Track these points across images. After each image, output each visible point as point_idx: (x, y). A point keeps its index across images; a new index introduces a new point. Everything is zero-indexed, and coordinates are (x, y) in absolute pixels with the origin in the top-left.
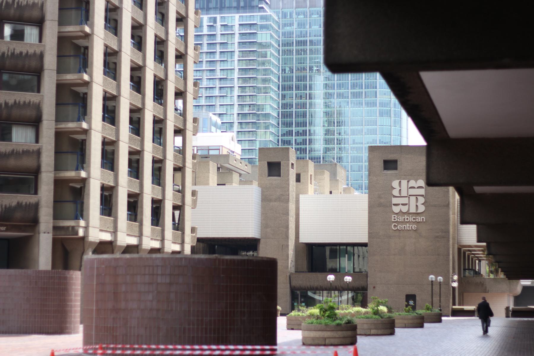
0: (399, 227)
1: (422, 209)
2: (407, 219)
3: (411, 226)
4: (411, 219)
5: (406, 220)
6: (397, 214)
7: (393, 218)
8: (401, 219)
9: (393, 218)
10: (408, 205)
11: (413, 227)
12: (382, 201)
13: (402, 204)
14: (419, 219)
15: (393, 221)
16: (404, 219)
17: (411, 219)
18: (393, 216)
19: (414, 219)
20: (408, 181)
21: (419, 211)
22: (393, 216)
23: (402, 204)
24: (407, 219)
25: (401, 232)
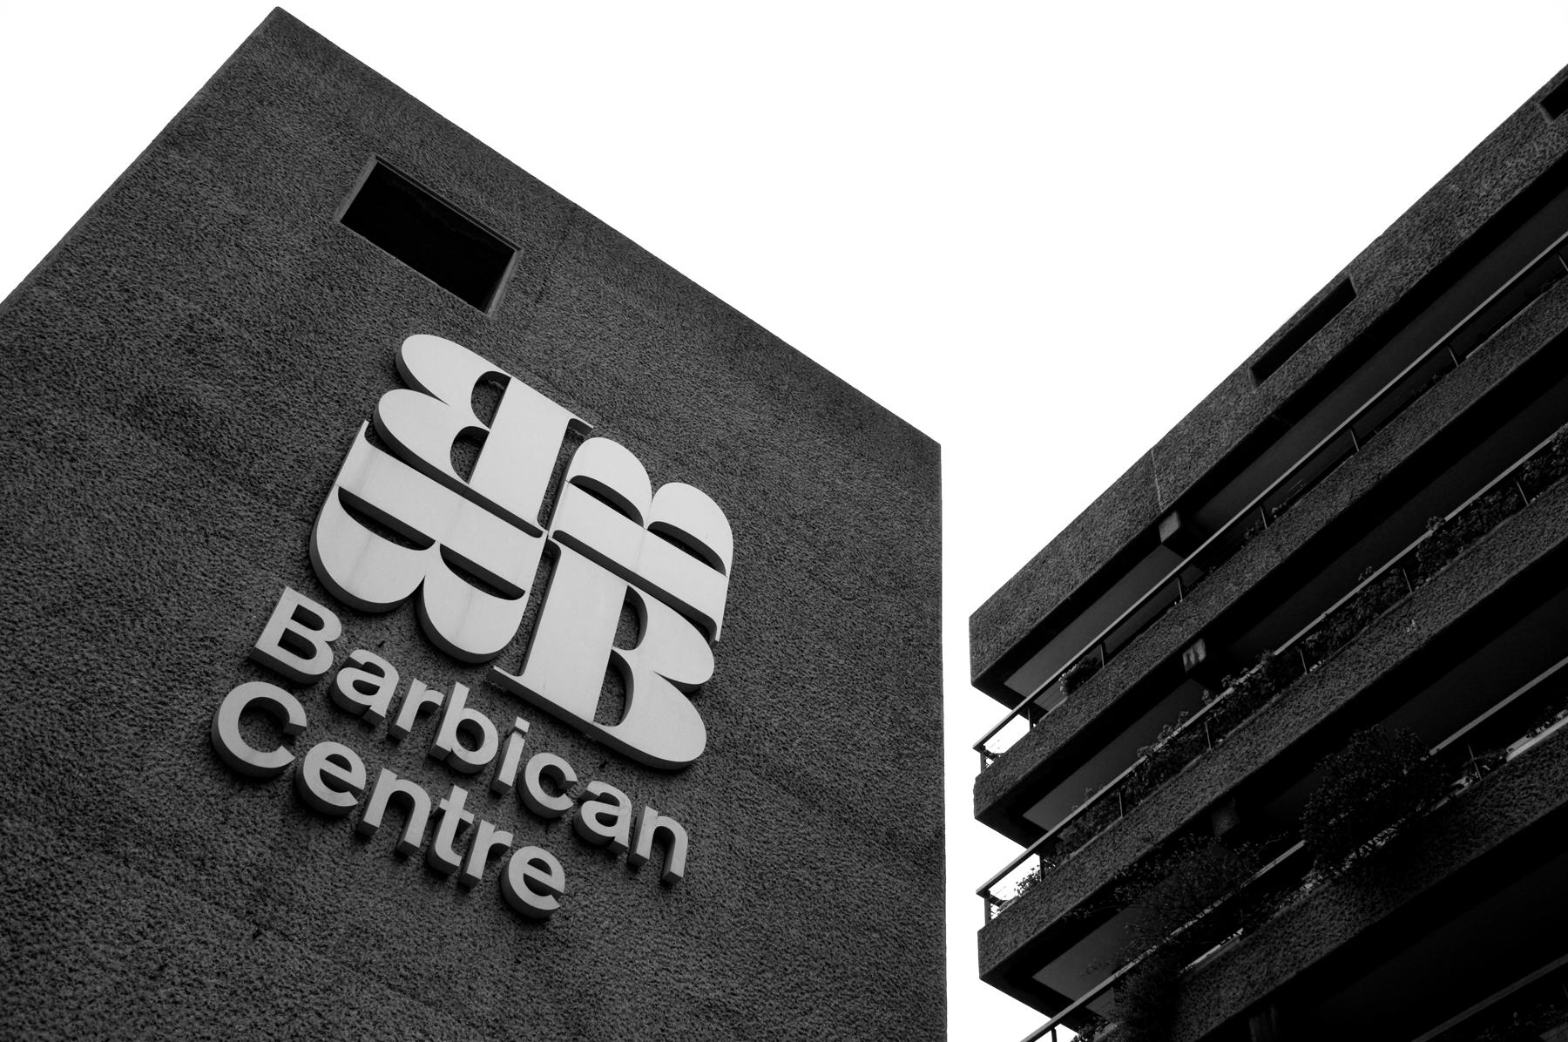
0: (315, 762)
1: (665, 728)
2: (470, 734)
3: (488, 835)
4: (517, 757)
5: (447, 739)
6: (353, 610)
7: (281, 620)
8: (391, 689)
9: (281, 620)
10: (566, 552)
11: (518, 868)
12: (207, 393)
13: (455, 562)
14: (618, 814)
15: (269, 643)
16: (430, 714)
17: (517, 757)
18: (291, 599)
19: (551, 779)
20: (575, 435)
21: (629, 732)
22: (291, 599)
23: (455, 562)
24: (470, 734)
25: (336, 839)
